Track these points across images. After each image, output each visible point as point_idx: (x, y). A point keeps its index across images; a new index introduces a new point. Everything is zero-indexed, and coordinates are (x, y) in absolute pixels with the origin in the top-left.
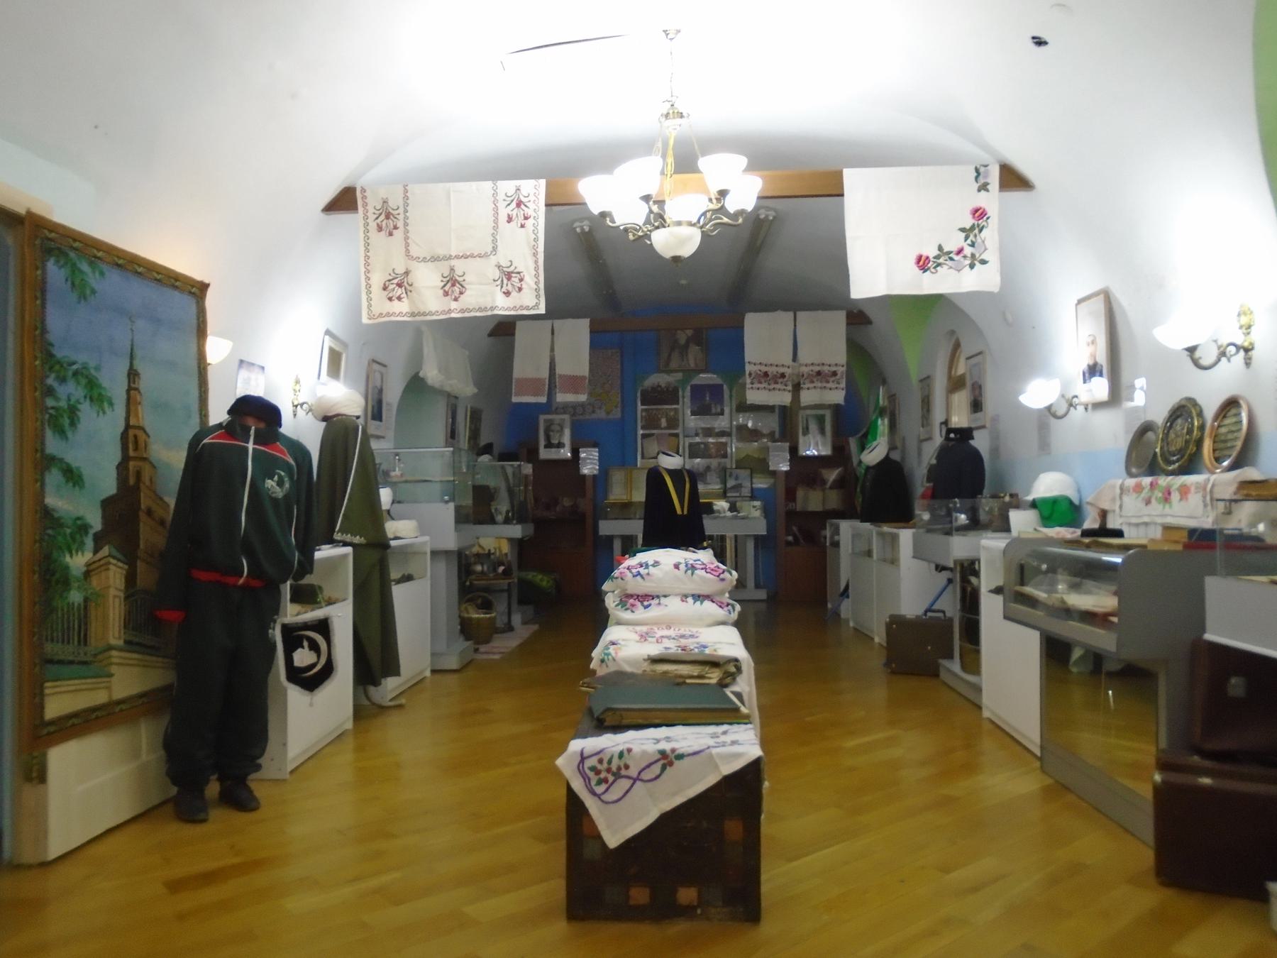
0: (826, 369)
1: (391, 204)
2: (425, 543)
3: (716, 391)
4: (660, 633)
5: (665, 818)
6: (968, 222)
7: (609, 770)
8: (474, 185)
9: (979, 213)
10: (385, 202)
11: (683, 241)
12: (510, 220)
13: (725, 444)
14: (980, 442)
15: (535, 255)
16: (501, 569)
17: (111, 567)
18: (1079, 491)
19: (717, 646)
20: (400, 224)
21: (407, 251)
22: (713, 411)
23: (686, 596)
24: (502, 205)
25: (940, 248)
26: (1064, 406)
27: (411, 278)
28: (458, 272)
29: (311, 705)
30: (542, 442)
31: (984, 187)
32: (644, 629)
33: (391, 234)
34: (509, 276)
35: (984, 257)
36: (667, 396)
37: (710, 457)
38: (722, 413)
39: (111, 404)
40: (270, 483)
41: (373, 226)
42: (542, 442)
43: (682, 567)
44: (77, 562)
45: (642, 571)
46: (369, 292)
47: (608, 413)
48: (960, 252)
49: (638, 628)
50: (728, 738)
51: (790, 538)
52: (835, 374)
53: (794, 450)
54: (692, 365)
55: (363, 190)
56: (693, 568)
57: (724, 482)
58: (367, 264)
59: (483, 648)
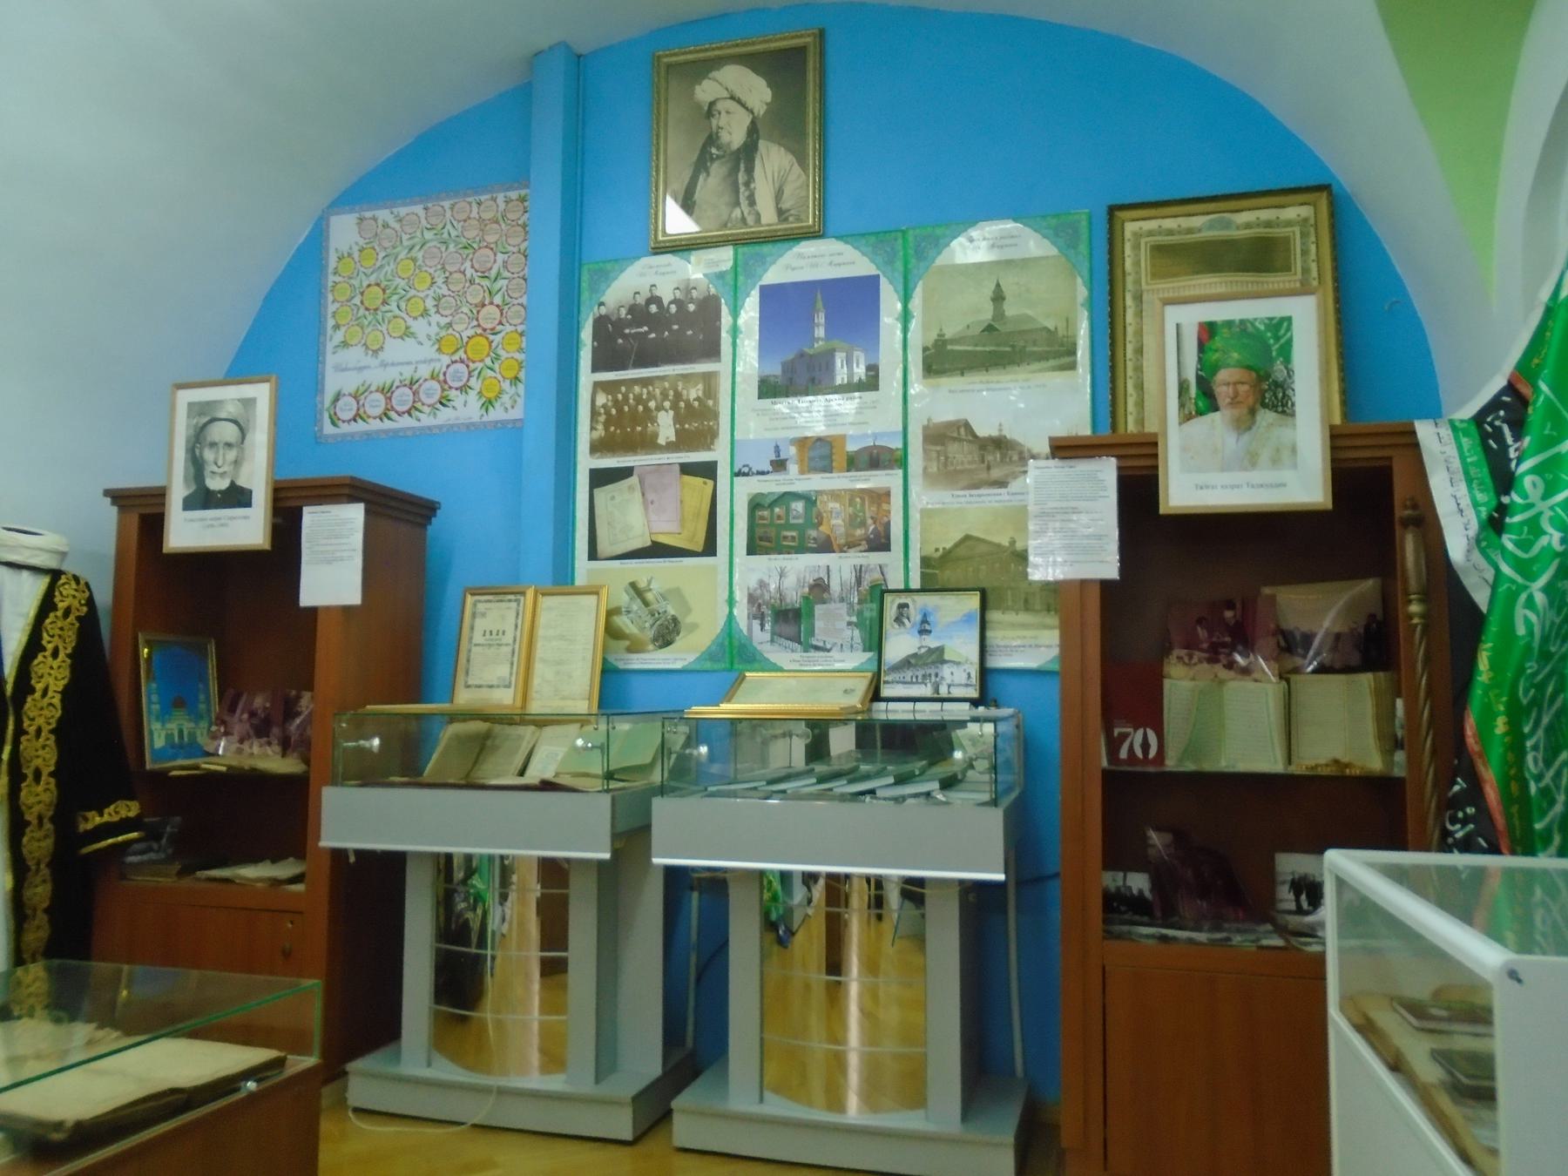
3: (852, 303)
13: (882, 496)
22: (841, 376)
30: (178, 492)
36: (686, 332)
37: (826, 546)
38: (871, 382)
42: (178, 492)
47: (488, 404)
51: (1139, 882)
54: (769, 216)
57: (875, 642)
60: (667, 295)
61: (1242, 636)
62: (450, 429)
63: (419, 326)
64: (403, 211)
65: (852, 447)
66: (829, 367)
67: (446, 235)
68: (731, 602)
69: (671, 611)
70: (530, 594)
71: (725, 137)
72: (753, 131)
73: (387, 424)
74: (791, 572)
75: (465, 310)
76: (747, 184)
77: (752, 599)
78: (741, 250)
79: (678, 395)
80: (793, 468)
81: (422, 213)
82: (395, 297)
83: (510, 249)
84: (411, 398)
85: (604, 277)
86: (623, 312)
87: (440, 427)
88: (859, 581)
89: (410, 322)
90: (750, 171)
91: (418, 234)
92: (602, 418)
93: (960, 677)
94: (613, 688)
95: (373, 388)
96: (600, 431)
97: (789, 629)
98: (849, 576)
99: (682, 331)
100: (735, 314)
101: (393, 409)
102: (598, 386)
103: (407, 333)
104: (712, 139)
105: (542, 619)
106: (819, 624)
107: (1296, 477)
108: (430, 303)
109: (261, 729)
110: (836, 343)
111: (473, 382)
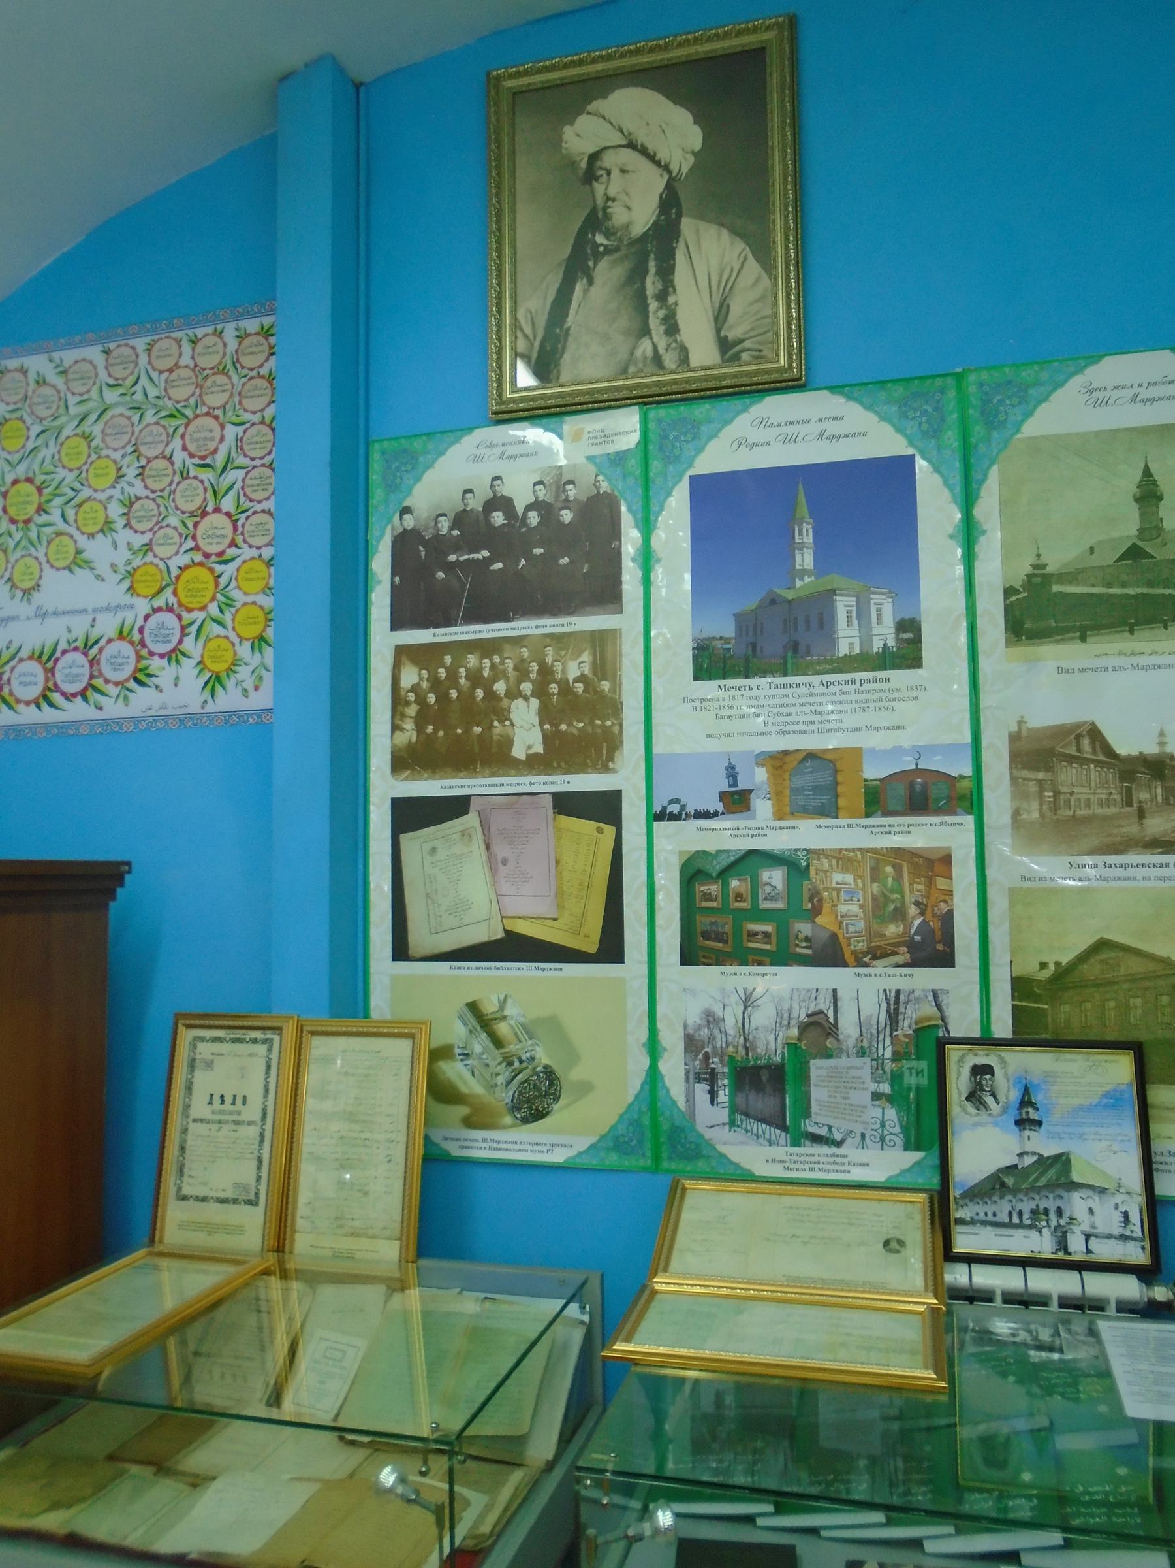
3: (866, 507)
13: (938, 864)
22: (847, 640)
37: (829, 954)
38: (907, 652)
47: (214, 683)
54: (703, 352)
57: (931, 1130)
60: (521, 490)
62: (151, 724)
63: (98, 549)
64: (69, 357)
65: (873, 771)
66: (825, 624)
67: (139, 396)
68: (653, 1047)
69: (543, 1058)
70: (290, 1029)
71: (619, 216)
72: (670, 202)
73: (48, 715)
74: (769, 999)
75: (173, 521)
76: (662, 297)
77: (691, 1044)
78: (655, 413)
79: (546, 672)
80: (763, 808)
81: (100, 360)
82: (58, 501)
83: (248, 417)
84: (86, 670)
85: (409, 464)
86: (444, 525)
87: (136, 721)
88: (894, 1018)
89: (83, 541)
90: (666, 272)
91: (94, 394)
92: (412, 710)
93: (1107, 1218)
94: (442, 1216)
95: (24, 653)
96: (409, 733)
97: (763, 1103)
98: (874, 1009)
99: (550, 558)
100: (647, 526)
101: (57, 688)
102: (402, 653)
103: (79, 561)
104: (596, 220)
105: (312, 1079)
106: (818, 1094)
108: (115, 510)
110: (836, 580)
111: (188, 644)
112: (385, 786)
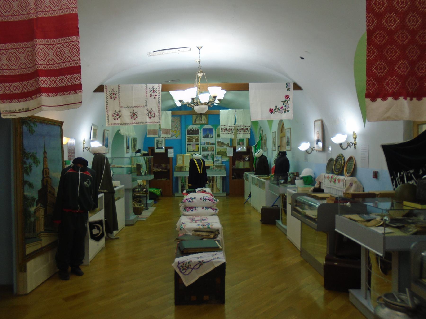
0: (245, 127)
1: (114, 90)
2: (123, 187)
3: (211, 130)
4: (197, 218)
5: (200, 278)
6: (284, 99)
7: (186, 267)
8: (140, 85)
9: (287, 97)
10: (113, 90)
11: (203, 109)
12: (151, 96)
13: (213, 147)
14: (289, 156)
15: (159, 107)
16: (145, 190)
17: (41, 209)
18: (315, 174)
19: (213, 224)
20: (117, 97)
21: (120, 105)
23: (203, 207)
24: (148, 92)
25: (276, 107)
26: (311, 150)
27: (121, 113)
28: (135, 111)
29: (98, 245)
30: (156, 147)
31: (289, 89)
32: (191, 217)
33: (115, 100)
34: (151, 113)
35: (289, 109)
37: (209, 151)
38: (212, 137)
39: (40, 163)
40: (85, 183)
41: (109, 97)
42: (156, 147)
43: (202, 199)
44: (32, 209)
45: (191, 200)
46: (108, 117)
48: (282, 108)
49: (190, 217)
50: (216, 256)
51: (233, 177)
52: (247, 129)
53: (235, 150)
55: (106, 86)
56: (205, 199)
57: (213, 159)
58: (107, 108)
59: (140, 216)
61: (241, 159)
74: (206, 153)
85: (188, 126)
107: (245, 149)
109: (157, 167)
112: (187, 143)
